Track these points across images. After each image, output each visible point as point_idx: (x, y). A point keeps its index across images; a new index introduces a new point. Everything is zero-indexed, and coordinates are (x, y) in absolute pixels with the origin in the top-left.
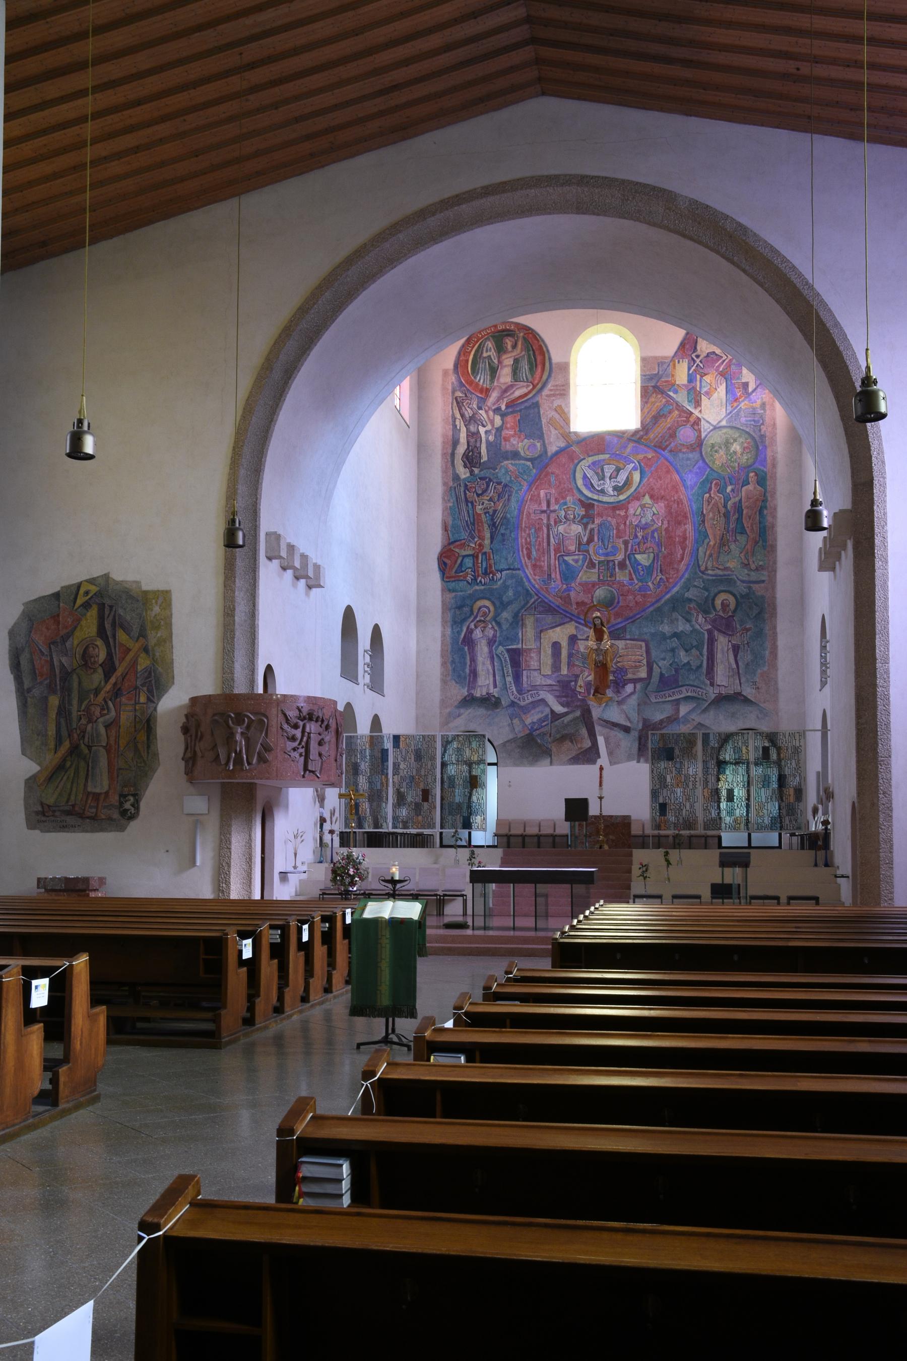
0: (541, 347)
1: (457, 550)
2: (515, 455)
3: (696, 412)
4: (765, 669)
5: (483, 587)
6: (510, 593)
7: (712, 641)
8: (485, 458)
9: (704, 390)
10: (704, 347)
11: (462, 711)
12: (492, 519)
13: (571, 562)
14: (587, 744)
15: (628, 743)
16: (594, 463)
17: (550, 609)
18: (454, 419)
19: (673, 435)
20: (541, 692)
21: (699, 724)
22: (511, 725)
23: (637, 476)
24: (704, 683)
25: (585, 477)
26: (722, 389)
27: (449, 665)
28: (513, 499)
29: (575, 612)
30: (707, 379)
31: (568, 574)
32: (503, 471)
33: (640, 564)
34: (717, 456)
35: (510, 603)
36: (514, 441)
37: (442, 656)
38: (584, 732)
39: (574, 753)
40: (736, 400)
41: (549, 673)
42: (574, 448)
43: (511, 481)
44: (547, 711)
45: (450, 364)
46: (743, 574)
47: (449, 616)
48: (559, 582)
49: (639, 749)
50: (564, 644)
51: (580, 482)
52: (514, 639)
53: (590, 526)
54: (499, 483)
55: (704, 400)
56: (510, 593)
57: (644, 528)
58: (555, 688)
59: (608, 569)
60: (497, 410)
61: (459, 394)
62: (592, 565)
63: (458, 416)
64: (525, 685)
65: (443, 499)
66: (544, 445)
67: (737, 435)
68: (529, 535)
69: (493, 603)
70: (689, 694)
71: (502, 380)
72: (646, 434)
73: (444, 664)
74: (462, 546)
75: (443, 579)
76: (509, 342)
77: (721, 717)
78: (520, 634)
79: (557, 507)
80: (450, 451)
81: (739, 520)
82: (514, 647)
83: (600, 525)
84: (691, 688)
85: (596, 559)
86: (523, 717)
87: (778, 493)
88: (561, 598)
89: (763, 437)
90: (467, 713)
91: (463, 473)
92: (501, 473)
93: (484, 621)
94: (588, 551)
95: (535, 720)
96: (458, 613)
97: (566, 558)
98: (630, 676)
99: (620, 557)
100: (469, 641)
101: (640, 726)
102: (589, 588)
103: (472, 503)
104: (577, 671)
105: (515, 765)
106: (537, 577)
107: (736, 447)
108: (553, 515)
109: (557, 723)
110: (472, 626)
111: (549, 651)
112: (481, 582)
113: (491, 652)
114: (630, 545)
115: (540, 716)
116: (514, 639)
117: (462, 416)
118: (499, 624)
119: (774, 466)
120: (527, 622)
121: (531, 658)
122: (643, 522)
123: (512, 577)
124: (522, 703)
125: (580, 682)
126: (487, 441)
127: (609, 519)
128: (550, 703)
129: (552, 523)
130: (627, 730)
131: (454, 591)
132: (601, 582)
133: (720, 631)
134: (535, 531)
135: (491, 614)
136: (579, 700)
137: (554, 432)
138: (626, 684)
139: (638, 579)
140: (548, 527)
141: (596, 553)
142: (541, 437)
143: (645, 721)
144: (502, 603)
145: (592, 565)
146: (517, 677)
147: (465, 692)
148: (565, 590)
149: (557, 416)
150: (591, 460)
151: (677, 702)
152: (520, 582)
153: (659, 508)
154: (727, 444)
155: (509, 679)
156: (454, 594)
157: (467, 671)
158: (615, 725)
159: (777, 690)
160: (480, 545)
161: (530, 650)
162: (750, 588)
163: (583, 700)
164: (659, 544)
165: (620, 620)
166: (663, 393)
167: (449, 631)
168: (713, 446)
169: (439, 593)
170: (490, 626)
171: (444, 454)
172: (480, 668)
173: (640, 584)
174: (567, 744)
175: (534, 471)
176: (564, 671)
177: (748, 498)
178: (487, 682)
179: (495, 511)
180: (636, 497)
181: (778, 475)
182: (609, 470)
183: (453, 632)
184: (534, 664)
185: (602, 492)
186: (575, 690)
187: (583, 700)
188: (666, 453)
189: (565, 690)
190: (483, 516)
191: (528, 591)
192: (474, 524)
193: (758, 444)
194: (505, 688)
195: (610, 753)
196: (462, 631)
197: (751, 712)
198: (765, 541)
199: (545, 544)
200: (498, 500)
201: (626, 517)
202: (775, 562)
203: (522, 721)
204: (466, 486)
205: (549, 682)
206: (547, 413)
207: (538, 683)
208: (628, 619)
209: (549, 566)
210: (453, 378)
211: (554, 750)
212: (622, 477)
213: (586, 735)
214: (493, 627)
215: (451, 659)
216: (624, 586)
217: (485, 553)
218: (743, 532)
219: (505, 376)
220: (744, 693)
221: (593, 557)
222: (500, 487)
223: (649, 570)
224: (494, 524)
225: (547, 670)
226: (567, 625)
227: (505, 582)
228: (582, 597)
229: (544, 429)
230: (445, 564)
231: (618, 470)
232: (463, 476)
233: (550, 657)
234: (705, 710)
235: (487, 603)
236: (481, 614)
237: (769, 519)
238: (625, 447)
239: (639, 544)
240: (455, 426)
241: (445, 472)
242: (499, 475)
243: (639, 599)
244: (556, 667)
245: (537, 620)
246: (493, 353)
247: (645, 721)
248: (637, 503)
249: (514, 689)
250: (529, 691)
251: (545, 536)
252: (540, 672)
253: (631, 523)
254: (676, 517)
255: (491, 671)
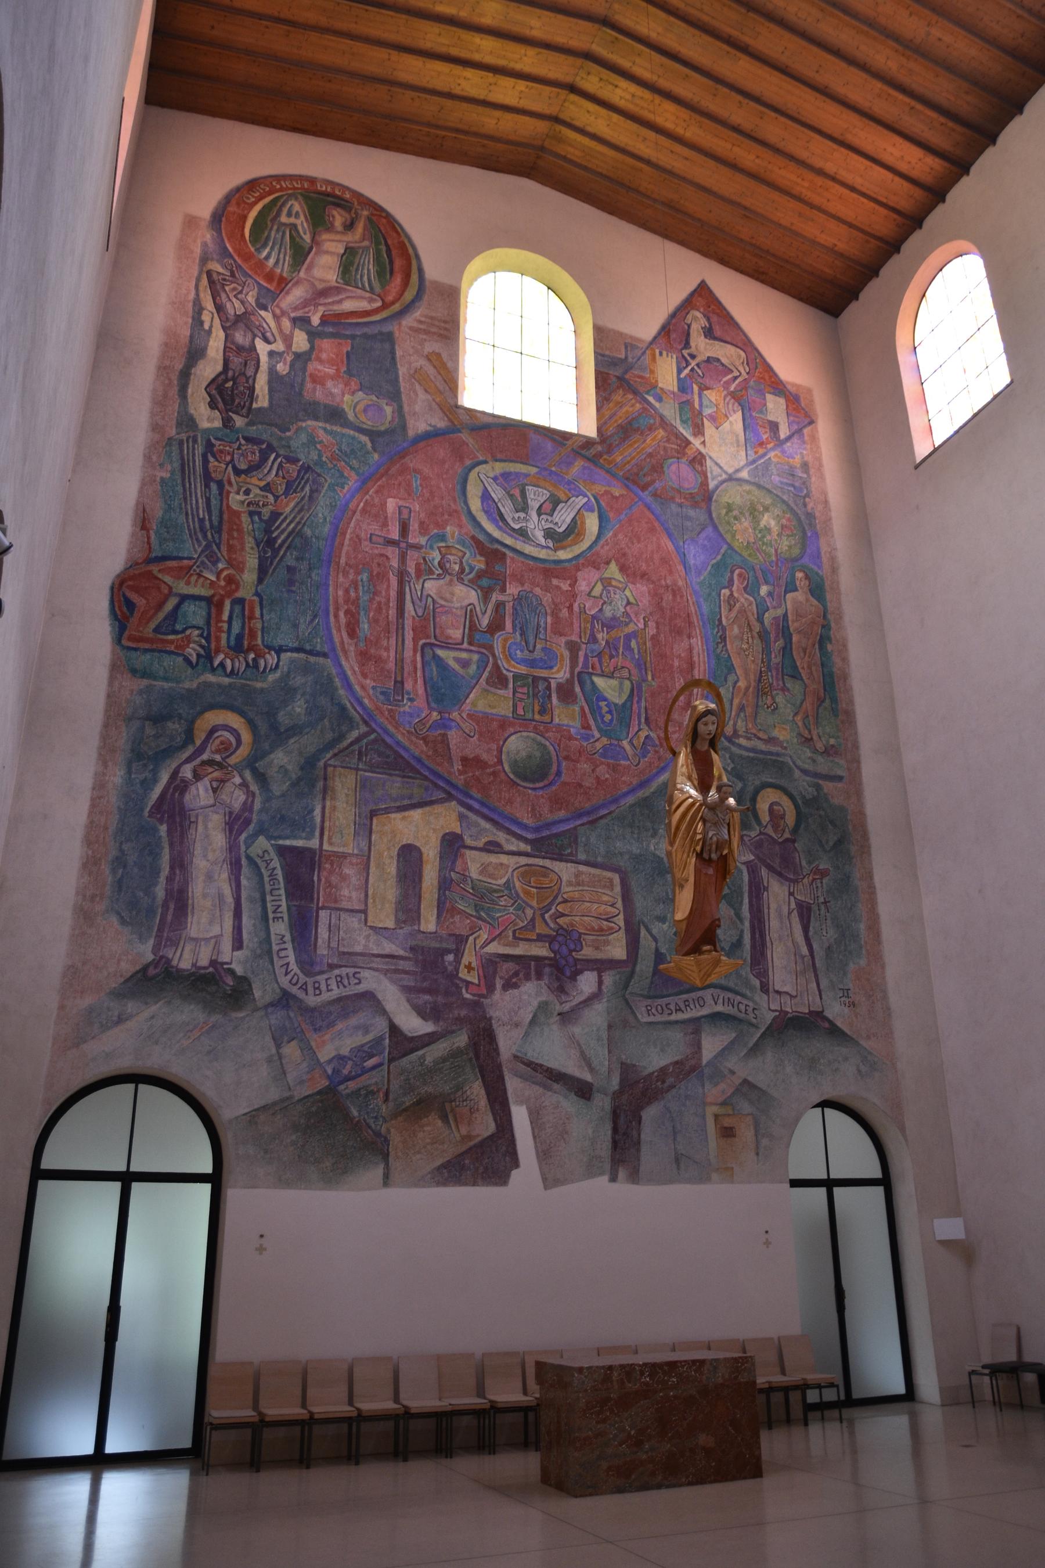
0: (402, 247)
1: (167, 579)
2: (335, 415)
3: (696, 442)
4: (863, 962)
5: (227, 681)
6: (299, 707)
7: (757, 890)
8: (262, 401)
9: (707, 411)
10: (702, 346)
11: (131, 1006)
12: (268, 531)
13: (452, 663)
14: (485, 1126)
15: (586, 1126)
16: (506, 476)
17: (396, 763)
18: (198, 308)
19: (658, 469)
20: (366, 974)
21: (745, 1081)
22: (278, 1062)
23: (592, 523)
24: (747, 983)
25: (486, 496)
26: (736, 420)
27: (106, 868)
28: (323, 500)
29: (460, 780)
30: (711, 396)
31: (445, 691)
32: (303, 438)
33: (605, 699)
34: (737, 526)
35: (295, 730)
36: (335, 388)
37: (89, 841)
38: (477, 1090)
39: (449, 1151)
40: (761, 444)
41: (390, 923)
42: (465, 436)
43: (320, 463)
44: (380, 1026)
45: (204, 208)
46: (803, 757)
47: (123, 738)
48: (421, 702)
49: (615, 1144)
50: (431, 853)
51: (475, 505)
52: (302, 824)
53: (495, 597)
54: (294, 461)
55: (709, 428)
56: (299, 707)
57: (610, 625)
58: (402, 965)
59: (535, 695)
60: (301, 322)
61: (216, 267)
62: (499, 679)
63: (209, 304)
64: (322, 950)
65: (147, 458)
66: (400, 411)
67: (768, 501)
68: (355, 584)
69: (251, 724)
70: (720, 1008)
71: (317, 273)
72: (610, 450)
73: (90, 864)
74: (183, 573)
75: (118, 640)
76: (339, 218)
77: (789, 1069)
78: (317, 812)
79: (423, 541)
80: (179, 366)
81: (787, 649)
82: (299, 843)
83: (519, 599)
84: (723, 994)
85: (511, 668)
86: (314, 1039)
87: (847, 619)
88: (424, 739)
89: (810, 516)
90: (145, 1014)
91: (207, 419)
92: (298, 441)
93: (220, 766)
94: (490, 648)
95: (345, 1051)
96: (150, 731)
97: (440, 652)
98: (587, 952)
99: (560, 674)
100: (173, 811)
101: (615, 1083)
102: (494, 729)
103: (220, 484)
104: (460, 925)
105: (288, 1184)
106: (368, 682)
107: (768, 520)
108: (413, 556)
109: (404, 1061)
110: (187, 772)
111: (392, 869)
112: (222, 665)
113: (232, 847)
114: (581, 654)
115: (360, 1039)
116: (302, 824)
117: (219, 308)
118: (262, 779)
119: (834, 570)
120: (338, 785)
121: (344, 878)
122: (608, 612)
123: (306, 669)
124: (312, 1000)
125: (469, 957)
126: (272, 372)
127: (538, 591)
128: (390, 1006)
129: (411, 570)
130: (583, 1091)
131: (145, 674)
132: (521, 722)
133: (771, 869)
134: (371, 579)
135: (243, 752)
136: (465, 1003)
137: (422, 396)
138: (580, 972)
139: (600, 730)
140: (402, 575)
141: (510, 657)
142: (395, 396)
143: (627, 1070)
144: (274, 727)
145: (499, 679)
146: (303, 927)
147: (146, 951)
148: (436, 725)
149: (431, 371)
150: (499, 467)
151: (695, 1026)
152: (326, 687)
153: (638, 592)
154: (754, 512)
155: (280, 928)
156: (145, 682)
157: (160, 892)
158: (556, 1077)
159: (888, 1010)
160: (230, 580)
161: (344, 856)
162: (818, 788)
163: (476, 1005)
164: (641, 665)
165: (562, 814)
166: (635, 393)
167: (117, 776)
168: (729, 508)
169: (102, 673)
170: (237, 780)
171: (163, 369)
172: (197, 888)
173: (605, 741)
174: (433, 1124)
175: (376, 456)
176: (429, 922)
177: (799, 616)
178: (216, 930)
179: (275, 515)
180: (592, 560)
181: (843, 587)
182: (536, 497)
183: (129, 781)
184: (349, 895)
185: (522, 533)
186: (453, 976)
187: (476, 1005)
188: (646, 495)
189: (430, 971)
190: (245, 518)
191: (343, 709)
192: (219, 531)
193: (806, 526)
194: (266, 951)
195: (544, 1155)
196: (155, 780)
197: (846, 1059)
198: (834, 700)
199: (392, 612)
200: (286, 493)
201: (573, 595)
202: (856, 746)
203: (309, 1051)
204: (209, 445)
205: (389, 948)
206: (410, 356)
207: (358, 949)
208: (580, 816)
209: (400, 662)
210: (209, 236)
211: (395, 1138)
212: (563, 517)
213: (483, 1102)
214: (244, 785)
215: (114, 853)
216: (570, 738)
217: (241, 601)
218: (796, 676)
219: (325, 267)
220: (828, 1014)
221: (503, 664)
222: (293, 469)
223: (624, 713)
224: (270, 542)
225: (384, 916)
226: (438, 809)
227: (287, 676)
228: (475, 747)
229: (403, 385)
230: (130, 605)
231: (555, 502)
232: (205, 424)
233: (392, 881)
234: (755, 1050)
235: (234, 720)
236: (214, 744)
237: (836, 660)
238: (570, 464)
239: (600, 655)
240: (198, 322)
241: (159, 403)
242: (294, 444)
243: (603, 772)
244: (408, 910)
245: (363, 785)
246: (302, 223)
247: (627, 1070)
248: (593, 575)
249: (292, 959)
250: (332, 967)
251: (393, 594)
252: (365, 916)
253: (583, 610)
254: (674, 621)
255: (230, 900)
